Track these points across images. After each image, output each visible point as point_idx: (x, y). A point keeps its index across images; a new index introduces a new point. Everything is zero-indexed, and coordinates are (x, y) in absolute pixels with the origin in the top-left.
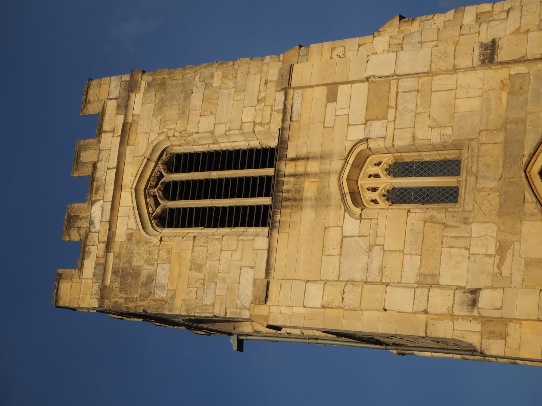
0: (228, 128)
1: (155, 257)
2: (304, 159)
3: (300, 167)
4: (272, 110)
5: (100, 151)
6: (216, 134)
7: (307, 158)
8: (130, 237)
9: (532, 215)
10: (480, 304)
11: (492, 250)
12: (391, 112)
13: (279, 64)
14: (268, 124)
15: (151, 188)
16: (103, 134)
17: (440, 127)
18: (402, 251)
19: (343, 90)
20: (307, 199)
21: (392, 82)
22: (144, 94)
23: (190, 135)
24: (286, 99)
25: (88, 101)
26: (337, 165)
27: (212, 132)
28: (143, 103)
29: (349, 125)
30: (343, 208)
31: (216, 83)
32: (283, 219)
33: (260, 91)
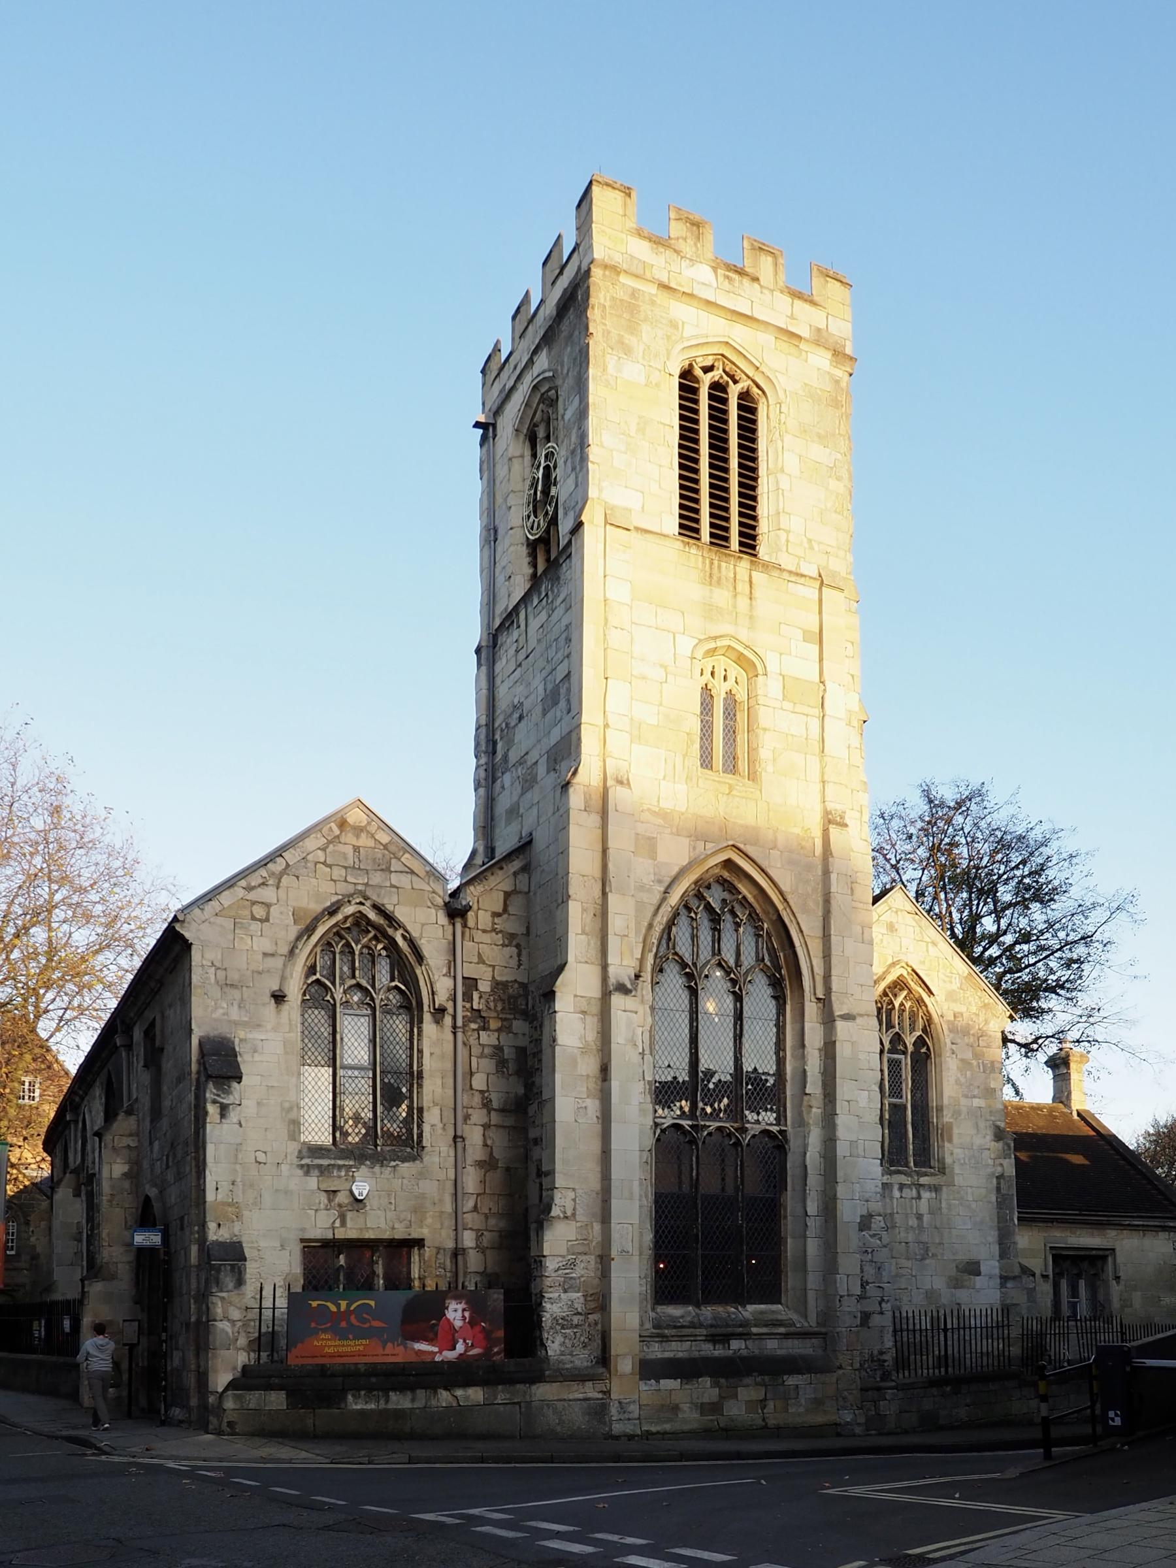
4: (799, 557)
5: (772, 291)
6: (779, 475)
8: (673, 324)
9: (694, 848)
10: (619, 788)
13: (843, 574)
15: (724, 363)
16: (790, 300)
17: (774, 760)
18: (661, 704)
21: (817, 710)
22: (829, 373)
24: (811, 578)
25: (828, 279)
27: (782, 470)
28: (819, 369)
29: (781, 654)
30: (702, 637)
31: (833, 484)
32: (693, 558)
33: (820, 543)
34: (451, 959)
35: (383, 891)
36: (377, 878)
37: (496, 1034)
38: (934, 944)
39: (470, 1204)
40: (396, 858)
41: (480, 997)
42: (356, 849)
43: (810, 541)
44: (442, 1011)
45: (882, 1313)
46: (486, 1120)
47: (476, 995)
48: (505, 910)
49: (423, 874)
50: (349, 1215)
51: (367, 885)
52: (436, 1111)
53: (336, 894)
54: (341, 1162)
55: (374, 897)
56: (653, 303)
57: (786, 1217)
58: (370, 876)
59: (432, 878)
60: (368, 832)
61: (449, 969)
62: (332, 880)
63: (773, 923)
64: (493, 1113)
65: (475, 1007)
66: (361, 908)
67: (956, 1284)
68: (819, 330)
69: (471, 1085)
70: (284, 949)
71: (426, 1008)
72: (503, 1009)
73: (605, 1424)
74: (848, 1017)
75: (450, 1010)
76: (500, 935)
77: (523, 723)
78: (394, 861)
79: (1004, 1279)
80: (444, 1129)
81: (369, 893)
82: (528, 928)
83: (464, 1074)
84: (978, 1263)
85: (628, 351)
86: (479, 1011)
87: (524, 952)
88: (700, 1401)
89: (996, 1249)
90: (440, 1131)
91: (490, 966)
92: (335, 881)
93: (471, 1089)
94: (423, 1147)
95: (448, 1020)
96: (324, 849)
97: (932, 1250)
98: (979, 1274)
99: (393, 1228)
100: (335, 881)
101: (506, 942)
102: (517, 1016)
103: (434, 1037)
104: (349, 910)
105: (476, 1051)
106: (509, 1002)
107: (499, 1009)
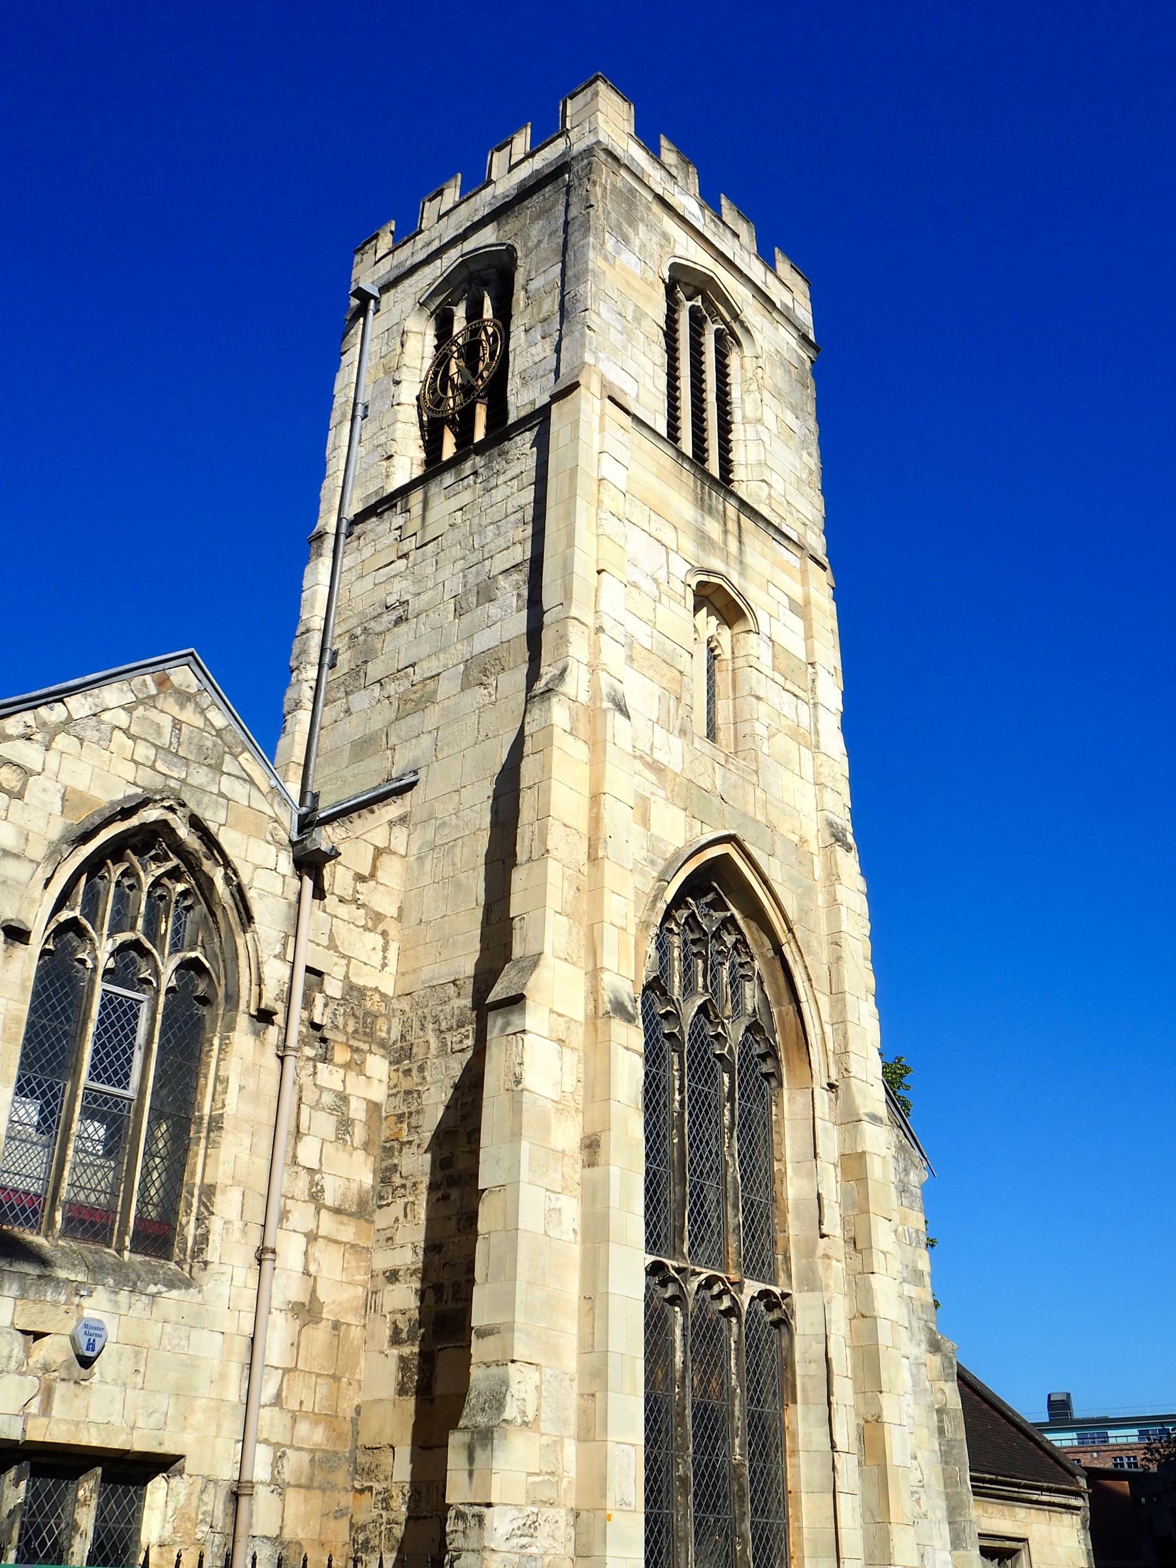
34: (292, 932)
35: (206, 799)
36: (200, 776)
37: (342, 1071)
41: (326, 1005)
42: (177, 724)
47: (319, 1000)
49: (265, 788)
51: (183, 782)
52: (235, 1195)
53: (135, 784)
55: (192, 805)
61: (285, 946)
65: (317, 1020)
66: (170, 816)
69: (295, 1157)
70: (38, 851)
71: (242, 1006)
72: (356, 1031)
76: (362, 911)
77: (404, 627)
78: (227, 758)
80: (244, 1232)
81: (185, 797)
82: (400, 909)
83: (289, 1133)
87: (394, 947)
90: (237, 1235)
91: (344, 956)
92: (137, 763)
93: (295, 1161)
94: (206, 1263)
95: (273, 1033)
100: (137, 763)
101: (370, 924)
102: (374, 1048)
103: (250, 1058)
104: (151, 814)
105: (309, 1096)
106: (365, 1022)
107: (350, 1029)
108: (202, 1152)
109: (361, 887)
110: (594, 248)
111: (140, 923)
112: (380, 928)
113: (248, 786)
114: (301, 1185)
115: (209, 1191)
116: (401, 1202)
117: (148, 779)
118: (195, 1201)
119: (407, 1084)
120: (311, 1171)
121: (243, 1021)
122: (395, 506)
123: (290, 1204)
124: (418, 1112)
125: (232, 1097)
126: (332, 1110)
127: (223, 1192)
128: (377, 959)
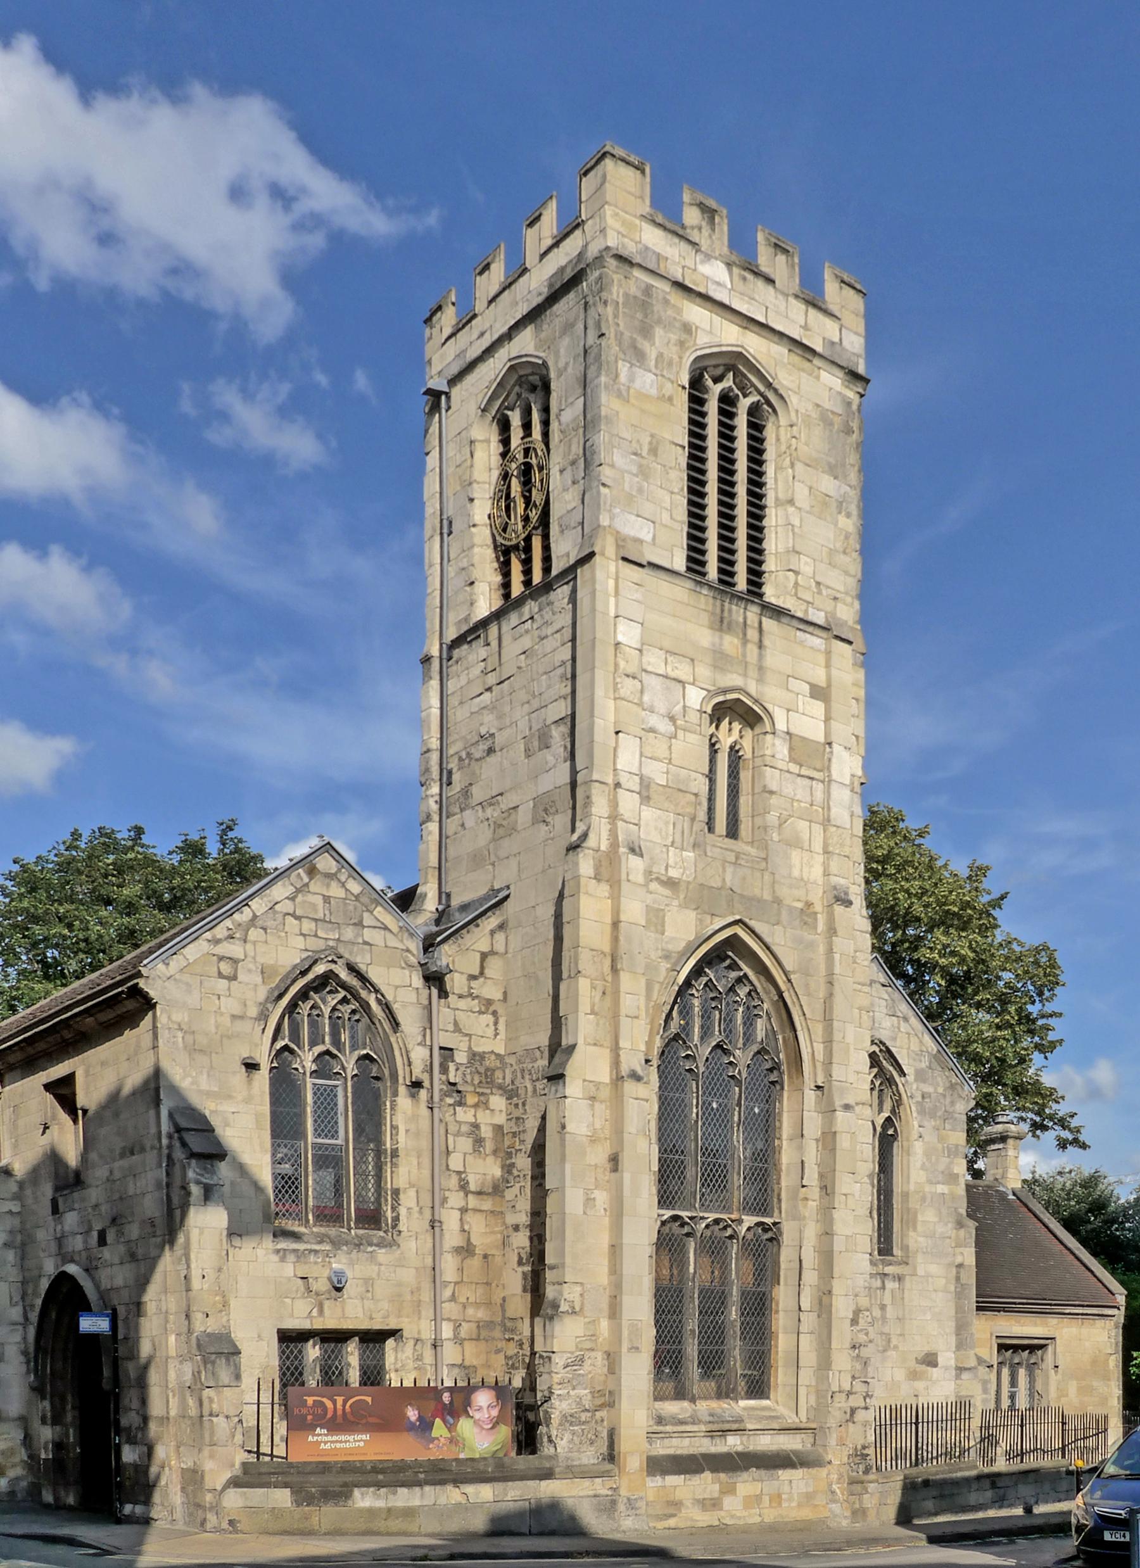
0: (796, 530)
1: (665, 373)
2: (760, 641)
3: (752, 634)
4: (808, 603)
7: (761, 646)
8: (687, 328)
11: (673, 873)
12: (794, 768)
13: (850, 623)
14: (796, 594)
19: (818, 708)
20: (721, 638)
22: (840, 393)
23: (792, 465)
26: (752, 688)
28: (831, 389)
29: (788, 710)
33: (828, 587)
35: (355, 949)
36: (349, 933)
37: (473, 1110)
38: (906, 1019)
39: (447, 1293)
40: (368, 910)
41: (457, 1070)
42: (327, 899)
43: (818, 584)
44: (417, 1085)
45: (866, 1408)
46: (462, 1204)
48: (482, 973)
49: (395, 929)
50: (327, 1304)
51: (338, 940)
52: (412, 1193)
53: (306, 950)
54: (317, 1247)
55: (346, 955)
56: (666, 302)
57: (777, 1312)
58: (343, 931)
59: (406, 935)
60: (339, 880)
61: (424, 1036)
62: (302, 934)
63: (774, 1003)
64: (470, 1197)
66: (332, 966)
67: (914, 1376)
68: (833, 343)
69: (447, 1166)
73: (614, 1519)
74: (847, 1107)
75: (426, 1084)
76: (476, 1001)
77: (492, 759)
78: (366, 915)
79: (960, 1370)
80: (421, 1212)
82: (505, 993)
83: (440, 1153)
84: (936, 1355)
85: (640, 356)
86: (454, 1084)
87: (502, 1021)
88: (701, 1497)
89: (953, 1340)
90: (416, 1215)
91: (467, 1035)
93: (448, 1169)
95: (423, 1094)
96: (292, 898)
97: (894, 1341)
98: (936, 1365)
99: (371, 1318)
101: (483, 1009)
102: (494, 1090)
103: (409, 1112)
104: (320, 969)
105: (452, 1128)
106: (486, 1075)
107: (476, 1082)
108: (389, 1170)
109: (474, 984)
110: (606, 387)
111: (327, 1039)
112: (491, 1009)
113: (383, 932)
114: (454, 1182)
115: (396, 1192)
116: (518, 1185)
117: (315, 944)
118: (389, 1198)
119: (518, 1113)
120: (459, 1173)
121: (402, 1090)
122: (479, 636)
123: (447, 1194)
124: (524, 1131)
125: (402, 1137)
126: (469, 1134)
127: (405, 1192)
128: (490, 1031)
